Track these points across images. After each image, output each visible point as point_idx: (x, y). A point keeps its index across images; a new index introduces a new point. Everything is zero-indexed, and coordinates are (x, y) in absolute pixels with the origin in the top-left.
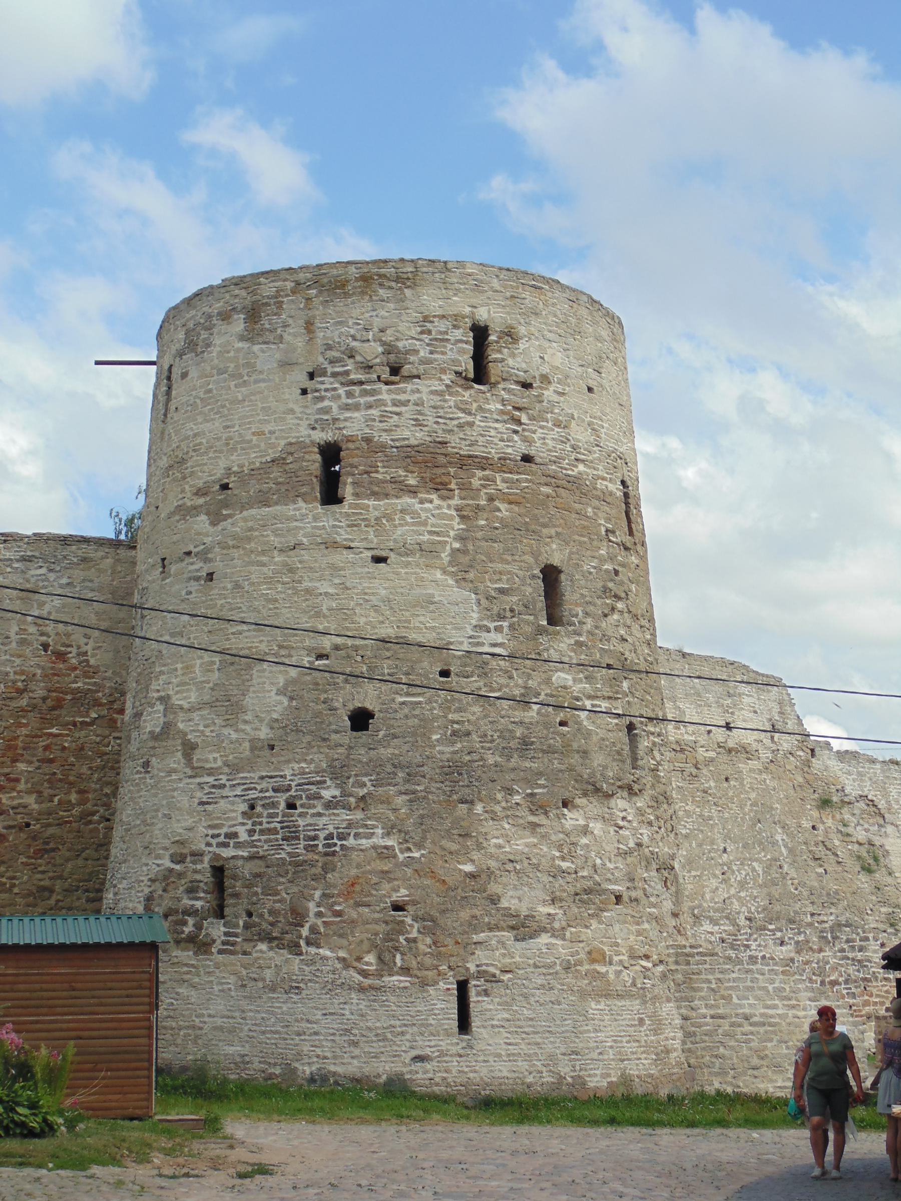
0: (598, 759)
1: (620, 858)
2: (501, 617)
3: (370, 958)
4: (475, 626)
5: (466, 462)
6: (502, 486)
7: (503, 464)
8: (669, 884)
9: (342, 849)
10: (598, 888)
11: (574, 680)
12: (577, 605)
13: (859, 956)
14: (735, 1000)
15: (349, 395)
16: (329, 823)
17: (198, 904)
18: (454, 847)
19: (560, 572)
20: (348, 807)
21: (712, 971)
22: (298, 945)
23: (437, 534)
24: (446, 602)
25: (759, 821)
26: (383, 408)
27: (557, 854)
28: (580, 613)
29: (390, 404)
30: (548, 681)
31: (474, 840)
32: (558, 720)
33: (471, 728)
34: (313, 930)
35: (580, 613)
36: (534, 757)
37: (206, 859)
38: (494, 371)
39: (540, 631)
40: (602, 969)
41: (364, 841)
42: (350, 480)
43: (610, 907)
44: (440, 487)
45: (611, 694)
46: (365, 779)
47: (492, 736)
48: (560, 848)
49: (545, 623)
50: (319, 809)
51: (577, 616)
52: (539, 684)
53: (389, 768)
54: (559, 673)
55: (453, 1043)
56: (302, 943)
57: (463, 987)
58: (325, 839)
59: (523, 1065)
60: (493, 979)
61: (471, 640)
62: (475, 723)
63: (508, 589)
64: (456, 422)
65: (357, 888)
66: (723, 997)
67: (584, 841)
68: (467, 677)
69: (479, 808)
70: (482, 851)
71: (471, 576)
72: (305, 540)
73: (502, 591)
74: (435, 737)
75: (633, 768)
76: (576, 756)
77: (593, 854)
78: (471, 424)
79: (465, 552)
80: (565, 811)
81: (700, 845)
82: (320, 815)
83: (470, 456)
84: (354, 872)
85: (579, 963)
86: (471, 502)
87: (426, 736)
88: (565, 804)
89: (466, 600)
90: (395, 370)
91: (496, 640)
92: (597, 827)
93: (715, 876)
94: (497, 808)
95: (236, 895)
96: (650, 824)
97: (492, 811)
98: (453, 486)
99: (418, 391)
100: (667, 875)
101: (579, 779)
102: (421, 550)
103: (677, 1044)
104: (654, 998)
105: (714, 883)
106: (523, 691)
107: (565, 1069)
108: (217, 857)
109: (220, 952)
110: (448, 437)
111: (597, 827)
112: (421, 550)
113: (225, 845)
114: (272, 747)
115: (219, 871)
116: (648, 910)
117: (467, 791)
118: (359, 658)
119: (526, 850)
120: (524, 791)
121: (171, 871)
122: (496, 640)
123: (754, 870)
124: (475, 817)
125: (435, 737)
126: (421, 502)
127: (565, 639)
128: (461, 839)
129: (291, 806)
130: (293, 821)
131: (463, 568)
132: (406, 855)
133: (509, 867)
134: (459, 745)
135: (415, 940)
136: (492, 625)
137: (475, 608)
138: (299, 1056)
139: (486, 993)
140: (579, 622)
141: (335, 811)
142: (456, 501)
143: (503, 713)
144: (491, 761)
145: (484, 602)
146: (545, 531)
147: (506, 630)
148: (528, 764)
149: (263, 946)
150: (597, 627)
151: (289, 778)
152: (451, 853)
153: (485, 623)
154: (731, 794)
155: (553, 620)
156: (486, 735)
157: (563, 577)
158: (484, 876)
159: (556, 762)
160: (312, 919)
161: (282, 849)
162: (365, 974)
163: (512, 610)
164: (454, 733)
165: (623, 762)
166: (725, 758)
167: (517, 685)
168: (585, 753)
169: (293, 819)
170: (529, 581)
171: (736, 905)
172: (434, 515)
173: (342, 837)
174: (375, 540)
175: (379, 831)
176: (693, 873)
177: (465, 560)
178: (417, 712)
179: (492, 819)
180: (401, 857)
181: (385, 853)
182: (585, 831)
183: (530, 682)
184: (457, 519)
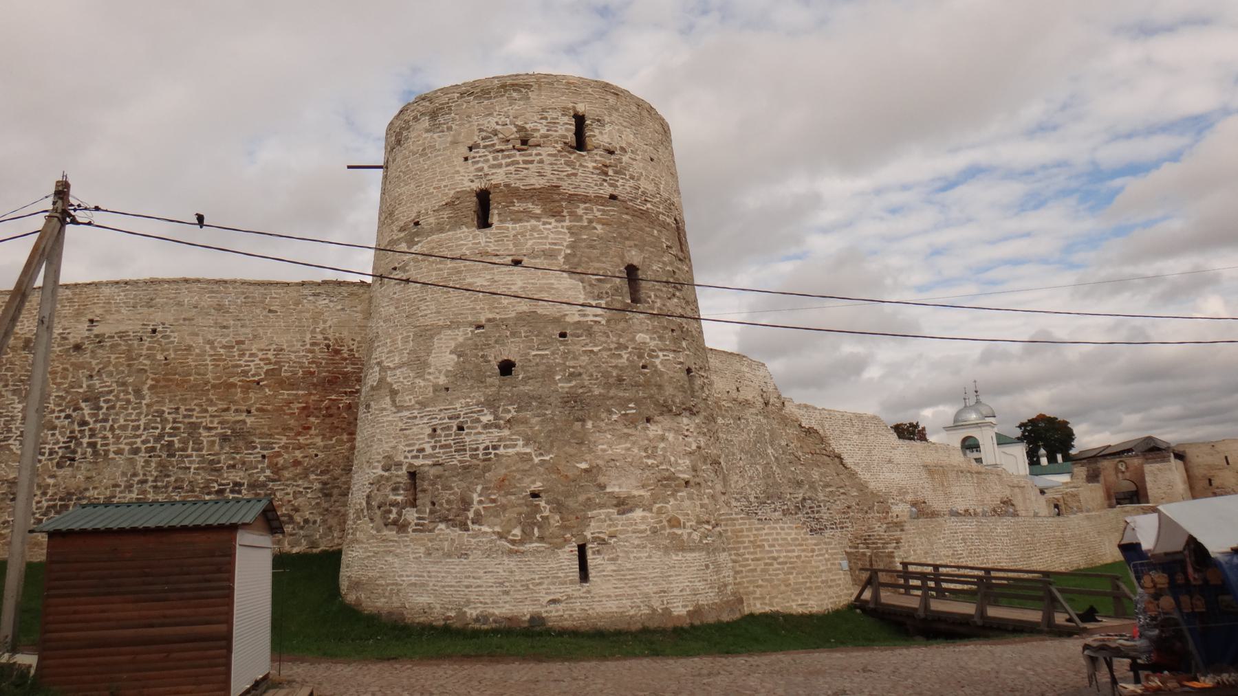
0: (669, 390)
3: (517, 531)
5: (572, 199)
6: (598, 214)
7: (598, 200)
13: (817, 516)
14: (767, 548)
15: (495, 159)
16: (485, 439)
17: (399, 498)
20: (498, 427)
21: (749, 530)
22: (466, 524)
23: (555, 244)
30: (633, 340)
34: (477, 513)
37: (404, 468)
38: (590, 142)
40: (679, 532)
41: (510, 450)
44: (557, 214)
48: (646, 450)
50: (480, 430)
55: (577, 590)
56: (469, 523)
57: (582, 549)
59: (628, 603)
60: (603, 542)
62: (584, 367)
65: (507, 482)
66: (759, 546)
67: (662, 445)
69: (589, 424)
74: (558, 377)
78: (575, 175)
79: (574, 255)
82: (480, 433)
84: (503, 471)
85: (663, 528)
87: (551, 377)
88: (648, 420)
90: (524, 142)
92: (670, 436)
95: (424, 491)
96: (704, 434)
103: (731, 580)
104: (715, 550)
105: (736, 478)
107: (656, 604)
108: (411, 465)
109: (414, 531)
110: (561, 183)
111: (670, 436)
113: (416, 457)
114: (447, 389)
115: (412, 475)
121: (382, 476)
125: (558, 377)
126: (544, 224)
129: (461, 428)
133: (612, 464)
134: (573, 383)
135: (547, 518)
138: (468, 603)
139: (599, 552)
142: (567, 223)
144: (596, 393)
148: (621, 394)
149: (442, 526)
155: (635, 300)
158: (594, 471)
160: (476, 506)
162: (513, 542)
166: (737, 407)
168: (660, 387)
171: (749, 490)
172: (553, 233)
173: (495, 448)
175: (521, 443)
180: (536, 460)
182: (663, 438)
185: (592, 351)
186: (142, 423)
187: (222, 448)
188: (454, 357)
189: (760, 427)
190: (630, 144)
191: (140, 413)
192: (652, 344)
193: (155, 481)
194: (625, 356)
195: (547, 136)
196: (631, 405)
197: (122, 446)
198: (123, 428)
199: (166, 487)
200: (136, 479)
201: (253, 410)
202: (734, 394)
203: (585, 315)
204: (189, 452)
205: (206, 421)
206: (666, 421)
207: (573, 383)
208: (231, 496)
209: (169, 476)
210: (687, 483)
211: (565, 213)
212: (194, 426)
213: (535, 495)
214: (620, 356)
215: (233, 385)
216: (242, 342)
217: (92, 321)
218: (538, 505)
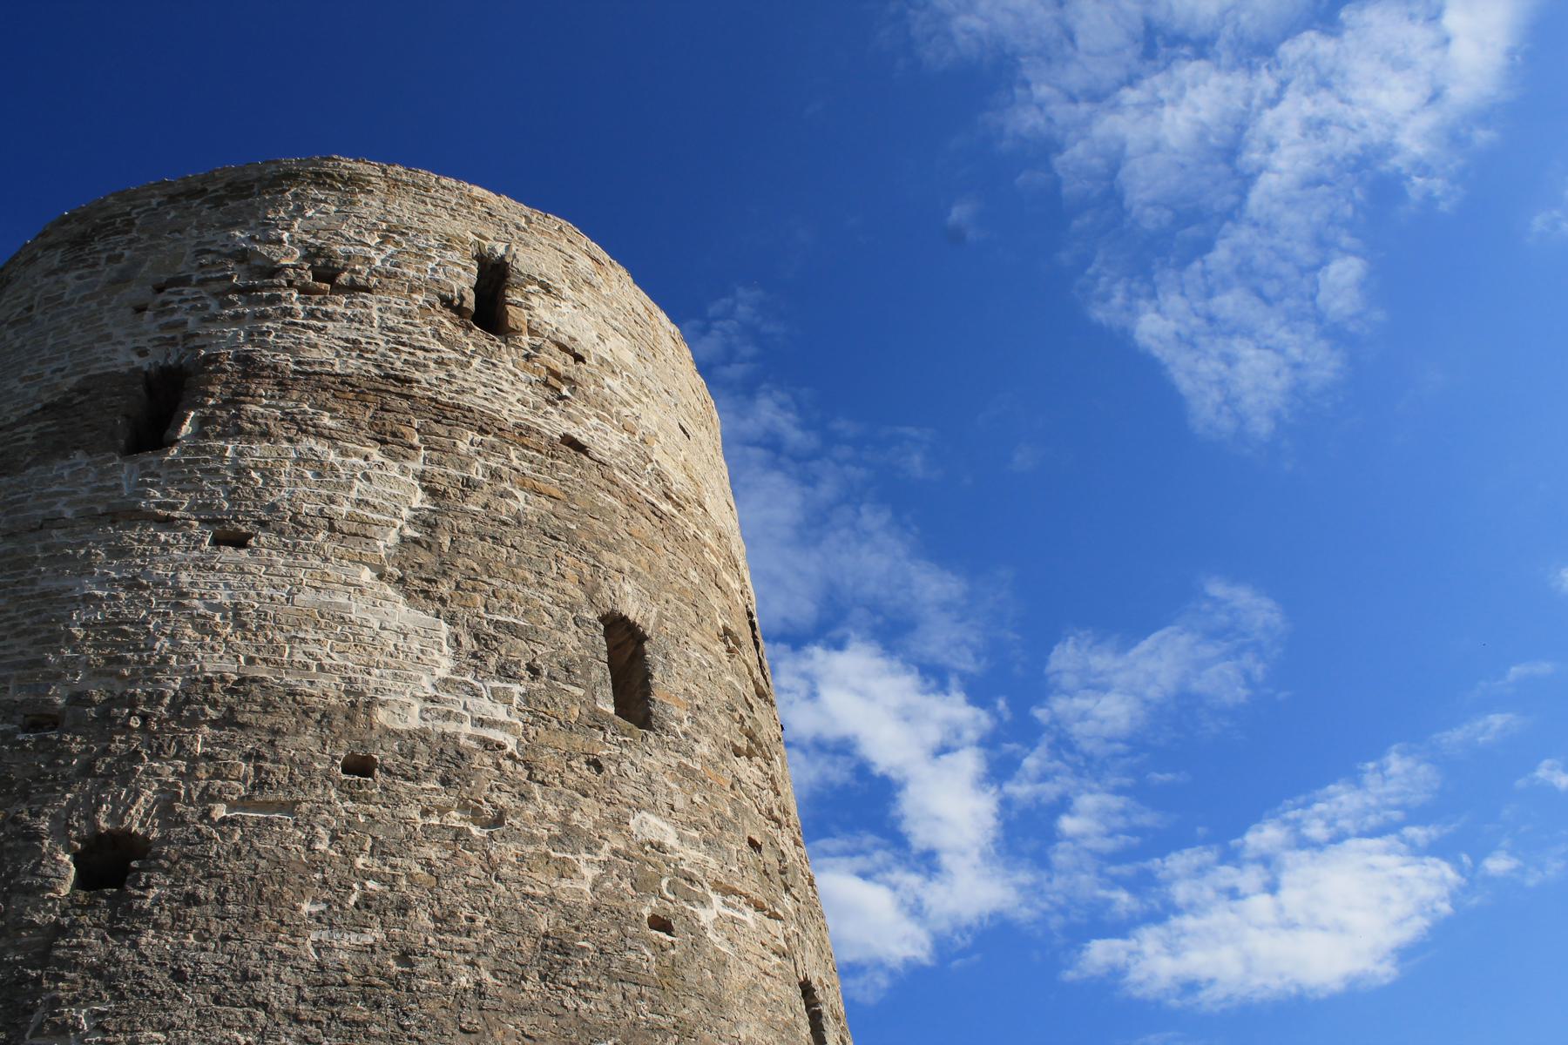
2: (504, 672)
4: (446, 681)
5: (447, 414)
19: (643, 638)
26: (288, 319)
30: (619, 823)
32: (646, 912)
36: (587, 986)
38: (516, 316)
39: (597, 722)
49: (611, 710)
51: (680, 721)
53: (160, 980)
61: (429, 705)
63: (525, 629)
64: (434, 355)
68: (417, 779)
71: (445, 588)
73: (511, 629)
76: (695, 1004)
86: (451, 471)
89: (428, 633)
98: (416, 441)
102: (332, 528)
106: (556, 831)
110: (417, 375)
112: (332, 528)
118: (135, 723)
122: (496, 713)
127: (656, 752)
134: (375, 934)
137: (446, 648)
142: (417, 465)
145: (466, 640)
146: (607, 556)
147: (516, 699)
153: (469, 678)
156: (453, 914)
157: (647, 646)
163: (534, 671)
164: (366, 901)
167: (541, 817)
177: (424, 557)
184: (420, 494)
190: (625, 367)
194: (590, 873)
195: (390, 275)
203: (447, 716)
207: (375, 934)
214: (565, 870)
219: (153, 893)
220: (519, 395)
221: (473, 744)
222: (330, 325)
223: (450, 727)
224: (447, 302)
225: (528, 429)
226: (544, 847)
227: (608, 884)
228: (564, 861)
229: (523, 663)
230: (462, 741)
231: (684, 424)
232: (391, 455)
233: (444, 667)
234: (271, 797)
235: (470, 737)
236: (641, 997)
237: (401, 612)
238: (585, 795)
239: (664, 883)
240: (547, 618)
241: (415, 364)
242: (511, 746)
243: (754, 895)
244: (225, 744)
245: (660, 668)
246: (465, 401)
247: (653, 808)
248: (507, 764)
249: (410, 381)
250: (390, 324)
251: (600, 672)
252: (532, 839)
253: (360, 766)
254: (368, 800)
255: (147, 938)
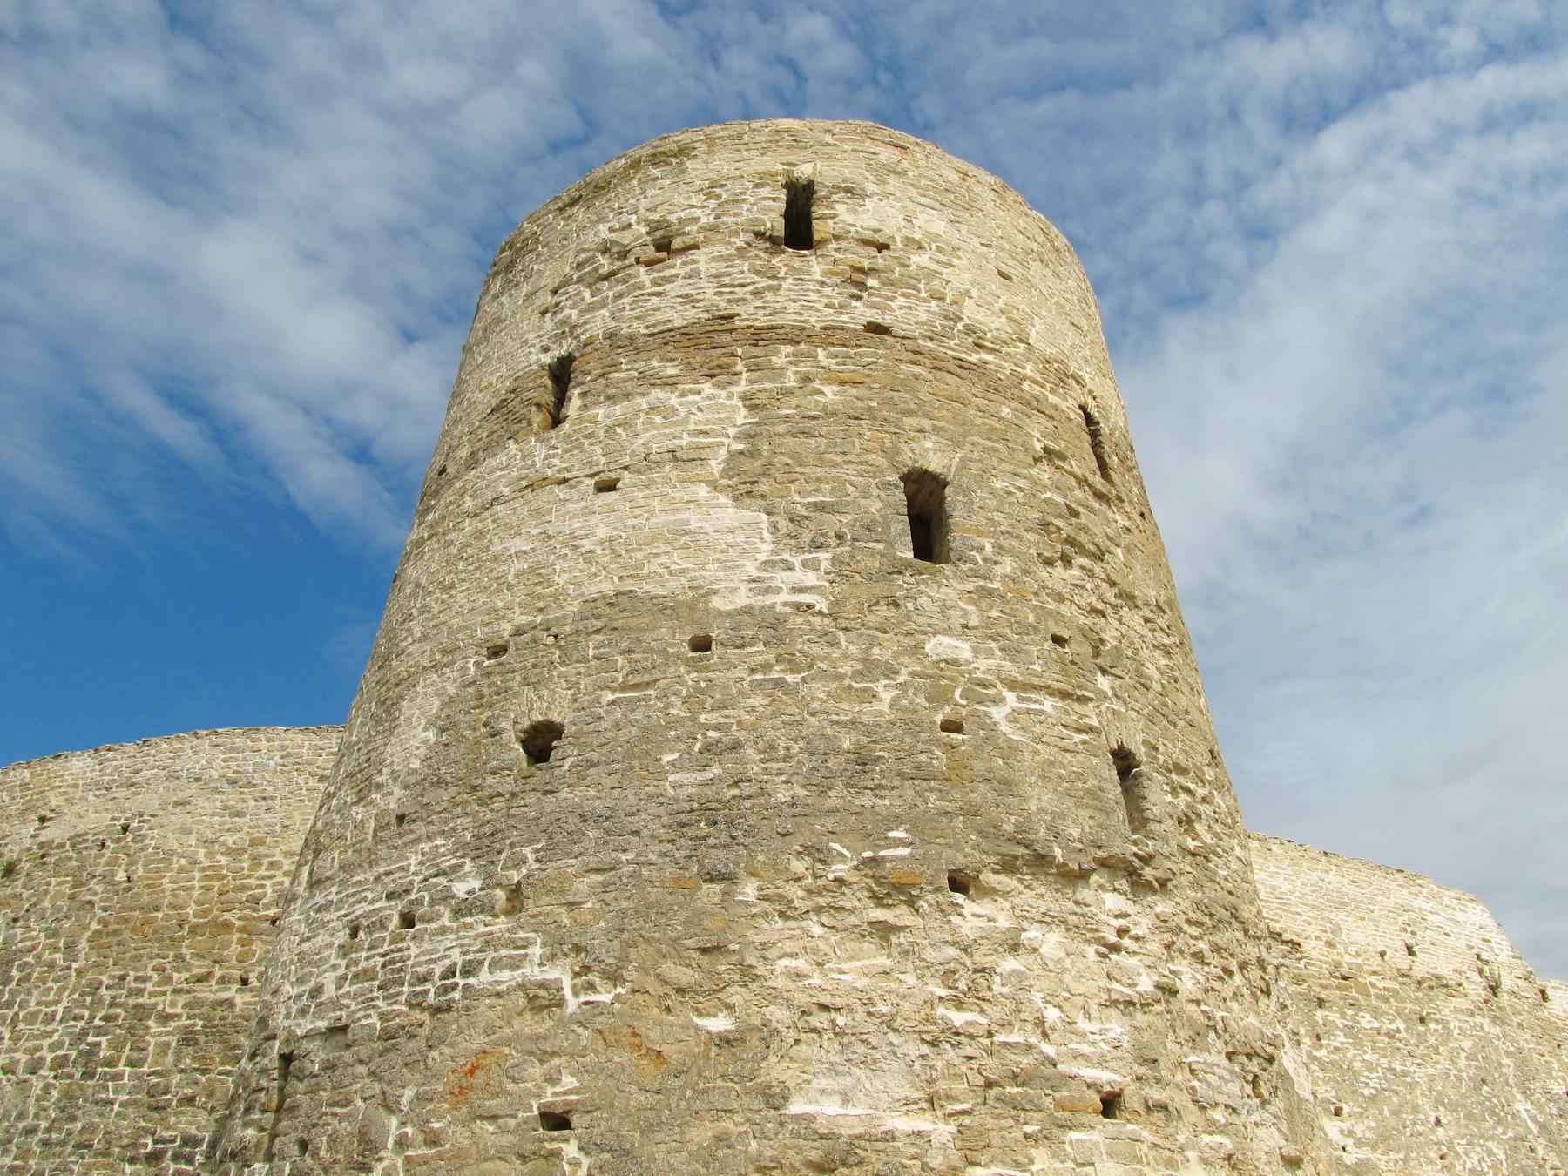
1: (1113, 1012)
4: (765, 562)
5: (759, 337)
6: (824, 361)
7: (831, 334)
8: (1264, 1090)
9: (464, 997)
10: (1049, 1070)
11: (976, 651)
12: (980, 533)
18: (686, 976)
24: (710, 530)
25: (1484, 1082)
27: (943, 992)
28: (988, 547)
29: (648, 284)
31: (734, 959)
32: (939, 718)
33: (742, 735)
35: (988, 547)
36: (880, 787)
38: (820, 229)
39: (899, 569)
41: (506, 974)
42: (577, 392)
43: (1086, 1119)
44: (719, 373)
45: (1069, 688)
46: (527, 851)
47: (787, 749)
48: (948, 976)
49: (910, 555)
51: (980, 549)
52: (896, 655)
53: (573, 823)
54: (939, 637)
58: (443, 977)
61: (753, 585)
63: (832, 504)
65: (480, 1078)
67: (1009, 964)
68: (743, 646)
69: (749, 890)
70: (755, 986)
71: (764, 487)
72: (506, 491)
73: (820, 507)
74: (667, 758)
75: (1134, 831)
76: (983, 787)
77: (1037, 998)
79: (753, 454)
80: (959, 898)
81: (1396, 1113)
82: (443, 931)
83: (773, 328)
86: (767, 385)
88: (958, 884)
89: (751, 526)
90: (664, 246)
91: (805, 580)
92: (1051, 943)
93: (1430, 1161)
94: (795, 891)
96: (1199, 957)
97: (779, 896)
98: (740, 367)
99: (694, 262)
100: (1256, 1070)
101: (992, 832)
102: (676, 459)
106: (859, 667)
110: (736, 309)
112: (676, 459)
116: (1206, 1138)
117: (722, 853)
119: (862, 983)
120: (856, 853)
122: (805, 580)
123: (1490, 1153)
124: (741, 911)
125: (667, 758)
126: (683, 395)
127: (955, 583)
128: (704, 960)
130: (401, 950)
131: (746, 481)
132: (583, 998)
133: (819, 1020)
134: (716, 770)
136: (797, 560)
137: (766, 535)
140: (984, 559)
141: (468, 920)
142: (743, 386)
143: (815, 706)
144: (783, 795)
145: (784, 525)
146: (909, 422)
147: (824, 566)
148: (866, 800)
150: (1026, 572)
151: (412, 869)
152: (680, 991)
153: (785, 556)
154: (1432, 1040)
156: (773, 748)
158: (754, 1041)
159: (933, 797)
161: (374, 1007)
163: (839, 536)
164: (708, 748)
165: (1107, 813)
166: (1409, 991)
167: (846, 657)
168: (1006, 785)
169: (403, 945)
170: (876, 492)
174: (603, 460)
175: (536, 951)
176: (1392, 1155)
178: (638, 715)
179: (782, 915)
180: (572, 1003)
181: (542, 1000)
183: (876, 651)
184: (744, 412)
185: (779, 683)
186: (61, 1008)
187: (179, 1058)
188: (431, 735)
189: (1483, 1043)
190: (935, 237)
191: (64, 988)
192: (982, 666)
193: (49, 1130)
194: (887, 696)
196: (899, 834)
197: (17, 1055)
198: (32, 1018)
199: (63, 1143)
200: (21, 1125)
201: (252, 977)
202: (1403, 961)
203: (768, 591)
204: (121, 1067)
205: (163, 1004)
206: (1037, 896)
207: (716, 770)
208: (173, 1167)
209: (73, 1119)
210: (1110, 1105)
211: (740, 367)
212: (141, 1013)
213: (557, 1121)
215: (228, 926)
216: (262, 842)
217: (43, 819)
218: (555, 1154)
219: (568, 763)
220: (825, 300)
221: (788, 609)
222: (668, 287)
223: (769, 600)
224: (759, 235)
225: (835, 328)
226: (847, 682)
227: (905, 702)
228: (866, 690)
229: (831, 533)
230: (779, 608)
231: (1004, 269)
232: (721, 386)
233: (765, 549)
234: (638, 679)
235: (785, 604)
236: (931, 790)
237: (729, 513)
238: (885, 632)
239: (957, 693)
240: (852, 489)
241: (737, 301)
242: (822, 605)
243: (1055, 685)
244: (609, 645)
245: (960, 506)
246: (778, 320)
247: (947, 631)
248: (817, 619)
249: (732, 317)
250: (714, 271)
251: (902, 525)
252: (841, 677)
253: (702, 645)
254: (707, 669)
255: (565, 793)
